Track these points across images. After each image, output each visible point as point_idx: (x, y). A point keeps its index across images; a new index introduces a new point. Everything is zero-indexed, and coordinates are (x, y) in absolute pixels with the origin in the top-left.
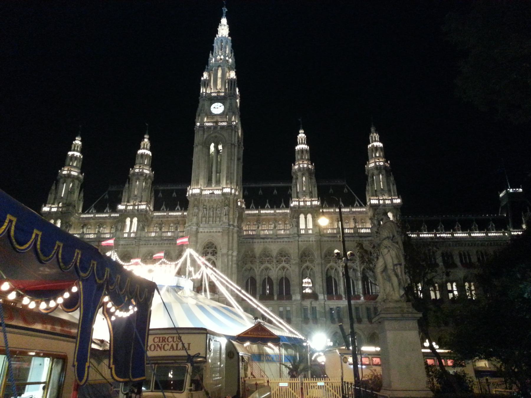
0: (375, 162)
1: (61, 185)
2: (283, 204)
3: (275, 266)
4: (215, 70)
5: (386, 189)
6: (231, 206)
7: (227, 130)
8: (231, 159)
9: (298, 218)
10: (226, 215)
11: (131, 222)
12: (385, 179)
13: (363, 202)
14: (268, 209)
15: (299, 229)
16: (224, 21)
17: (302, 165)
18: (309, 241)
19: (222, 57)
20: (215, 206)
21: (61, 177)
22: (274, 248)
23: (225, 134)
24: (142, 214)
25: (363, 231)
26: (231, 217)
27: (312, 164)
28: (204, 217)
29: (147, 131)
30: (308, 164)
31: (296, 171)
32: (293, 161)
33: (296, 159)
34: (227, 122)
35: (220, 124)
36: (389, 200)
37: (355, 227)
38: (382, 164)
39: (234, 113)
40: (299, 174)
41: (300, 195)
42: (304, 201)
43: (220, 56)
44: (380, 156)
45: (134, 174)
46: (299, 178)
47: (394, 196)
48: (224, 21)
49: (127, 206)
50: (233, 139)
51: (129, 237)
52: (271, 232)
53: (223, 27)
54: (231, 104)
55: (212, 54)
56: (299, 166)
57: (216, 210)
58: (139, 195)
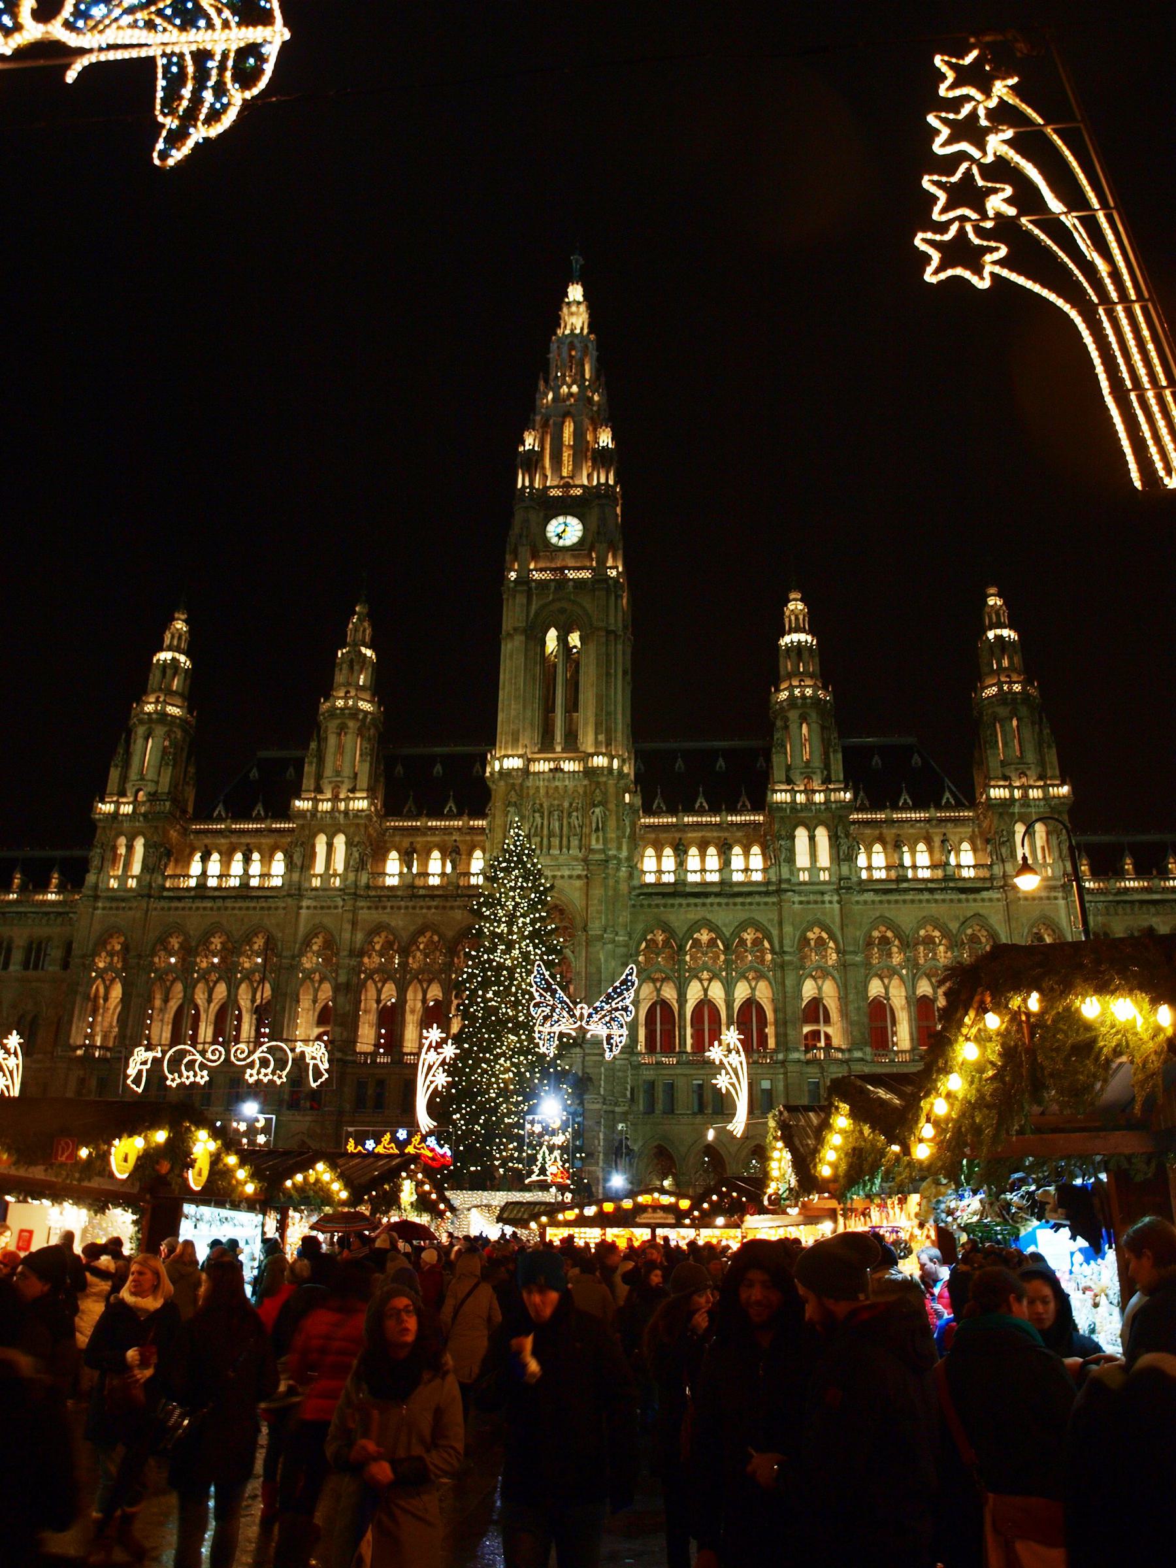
0: (999, 684)
1: (140, 741)
2: (744, 798)
4: (555, 424)
5: (1031, 757)
6: (612, 806)
7: (594, 590)
8: (608, 674)
9: (793, 838)
10: (597, 829)
11: (330, 846)
12: (1027, 733)
13: (968, 796)
14: (701, 812)
15: (794, 870)
16: (575, 292)
17: (797, 689)
18: (823, 902)
19: (575, 389)
20: (566, 804)
23: (587, 603)
24: (358, 825)
26: (612, 835)
27: (825, 688)
28: (536, 835)
30: (815, 688)
31: (782, 708)
32: (774, 680)
33: (782, 672)
34: (593, 569)
35: (571, 575)
36: (1038, 787)
38: (1017, 688)
39: (612, 547)
40: (793, 715)
41: (796, 776)
42: (805, 791)
43: (569, 387)
44: (1012, 668)
46: (793, 727)
48: (575, 292)
49: (316, 801)
50: (612, 620)
51: (325, 889)
53: (574, 309)
54: (603, 520)
55: (546, 382)
56: (792, 694)
57: (570, 815)
58: (347, 772)
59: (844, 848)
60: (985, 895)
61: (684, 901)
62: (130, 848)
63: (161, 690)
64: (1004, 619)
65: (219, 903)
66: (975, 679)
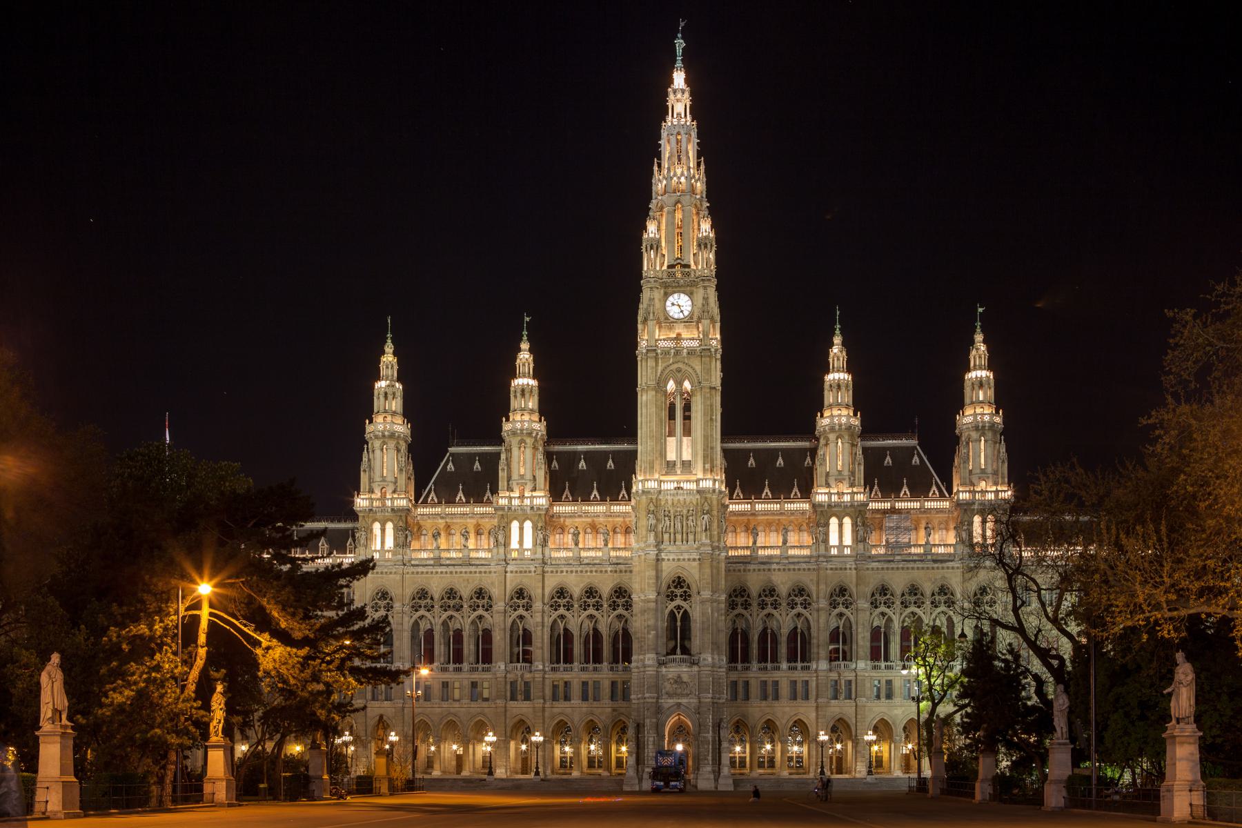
1: (378, 452)
3: (784, 614)
5: (989, 470)
9: (827, 525)
11: (521, 529)
12: (989, 451)
15: (828, 548)
17: (837, 414)
21: (377, 437)
22: (783, 583)
25: (941, 550)
29: (525, 333)
33: (826, 403)
37: (927, 543)
38: (987, 418)
40: (832, 437)
41: (832, 481)
45: (514, 433)
46: (832, 445)
47: (1003, 483)
52: (777, 552)
58: (529, 476)
59: (861, 533)
60: (950, 564)
61: (756, 567)
62: (383, 530)
63: (386, 411)
64: (984, 362)
65: (451, 569)
66: (959, 405)
